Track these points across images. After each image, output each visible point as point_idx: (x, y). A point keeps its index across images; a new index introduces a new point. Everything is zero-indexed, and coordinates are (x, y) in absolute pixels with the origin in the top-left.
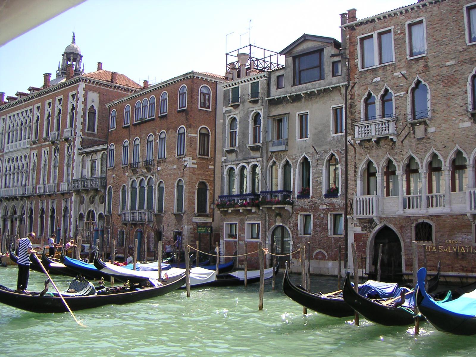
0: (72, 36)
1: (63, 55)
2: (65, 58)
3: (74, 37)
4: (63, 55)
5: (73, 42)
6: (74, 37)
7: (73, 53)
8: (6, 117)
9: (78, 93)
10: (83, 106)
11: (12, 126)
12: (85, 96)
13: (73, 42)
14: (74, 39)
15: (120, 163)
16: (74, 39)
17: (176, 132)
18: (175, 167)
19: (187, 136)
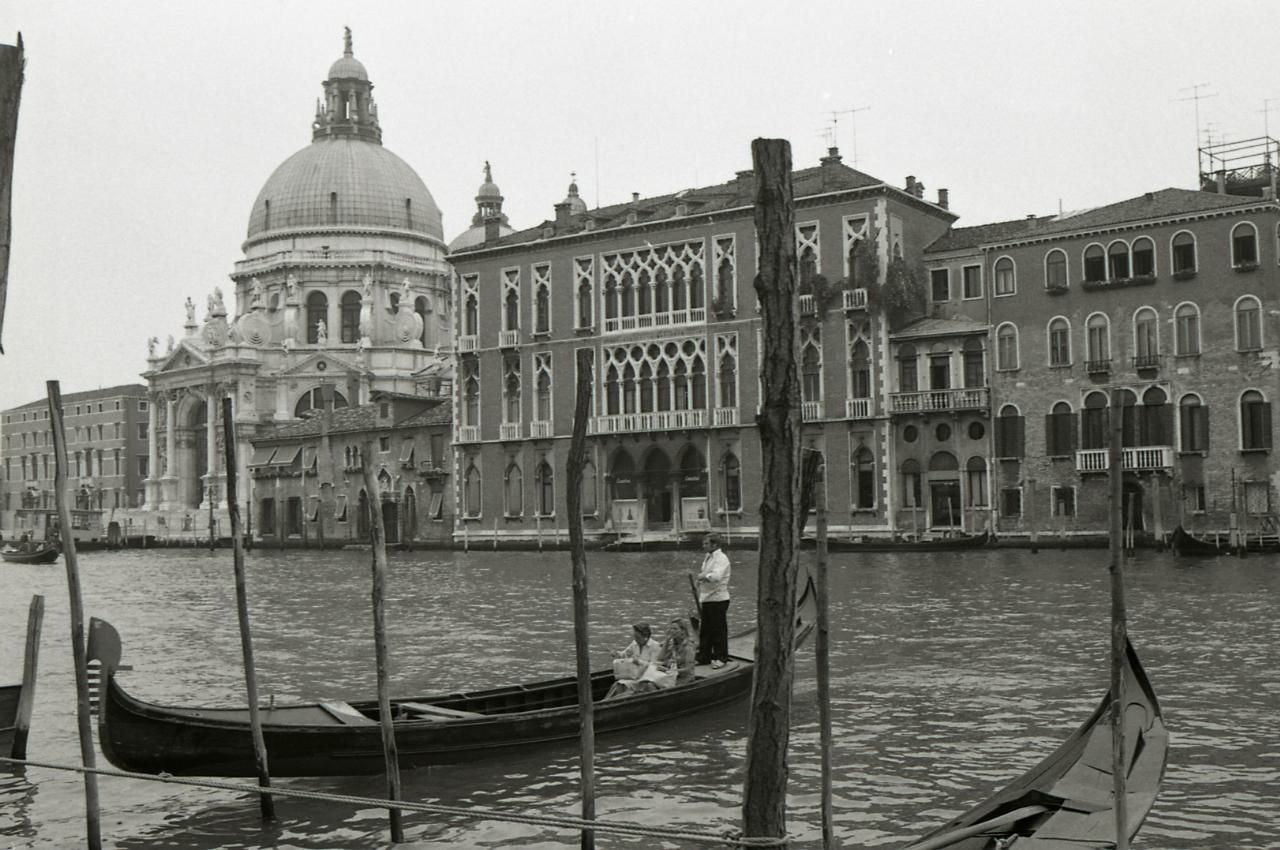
0: (344, 35)
1: (325, 84)
2: (336, 92)
3: (349, 38)
4: (325, 84)
5: (348, 51)
6: (349, 38)
7: (355, 81)
8: (597, 257)
9: (874, 218)
10: (886, 243)
11: (619, 278)
12: (888, 225)
13: (348, 51)
14: (349, 44)
15: (1044, 359)
16: (349, 44)
17: (1231, 306)
18: (1234, 368)
19: (1267, 315)
